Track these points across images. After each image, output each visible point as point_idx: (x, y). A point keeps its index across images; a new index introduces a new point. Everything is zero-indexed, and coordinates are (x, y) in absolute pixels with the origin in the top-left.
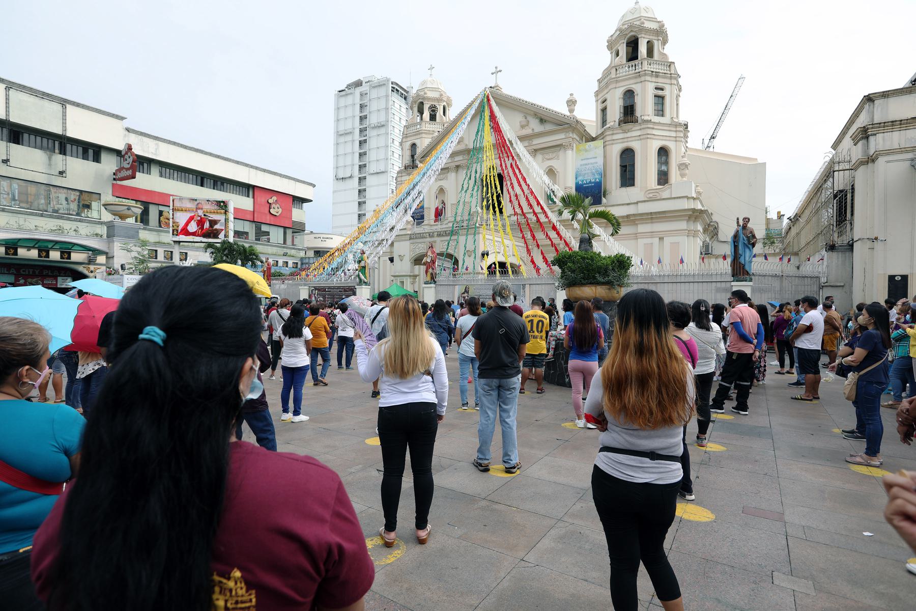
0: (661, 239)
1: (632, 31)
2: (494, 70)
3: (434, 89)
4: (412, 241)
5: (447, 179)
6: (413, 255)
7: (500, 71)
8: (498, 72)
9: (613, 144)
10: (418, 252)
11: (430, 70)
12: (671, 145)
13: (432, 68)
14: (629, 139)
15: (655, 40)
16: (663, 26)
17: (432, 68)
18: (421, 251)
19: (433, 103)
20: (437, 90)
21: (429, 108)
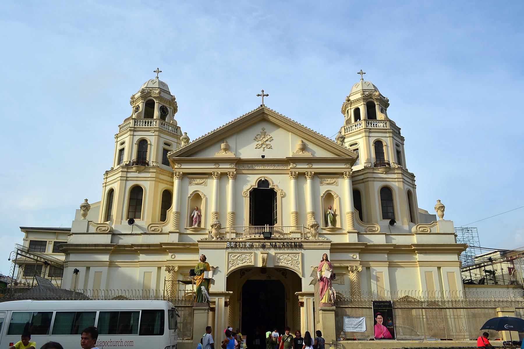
0: (439, 268)
1: (371, 98)
2: (261, 93)
3: (166, 92)
4: (230, 250)
5: (206, 185)
6: (233, 268)
7: (268, 95)
8: (264, 96)
9: (374, 181)
10: (240, 265)
11: (156, 74)
12: (411, 189)
13: (158, 71)
14: (387, 179)
15: (384, 109)
16: (388, 101)
17: (158, 71)
18: (245, 264)
19: (165, 105)
20: (168, 93)
21: (160, 108)
